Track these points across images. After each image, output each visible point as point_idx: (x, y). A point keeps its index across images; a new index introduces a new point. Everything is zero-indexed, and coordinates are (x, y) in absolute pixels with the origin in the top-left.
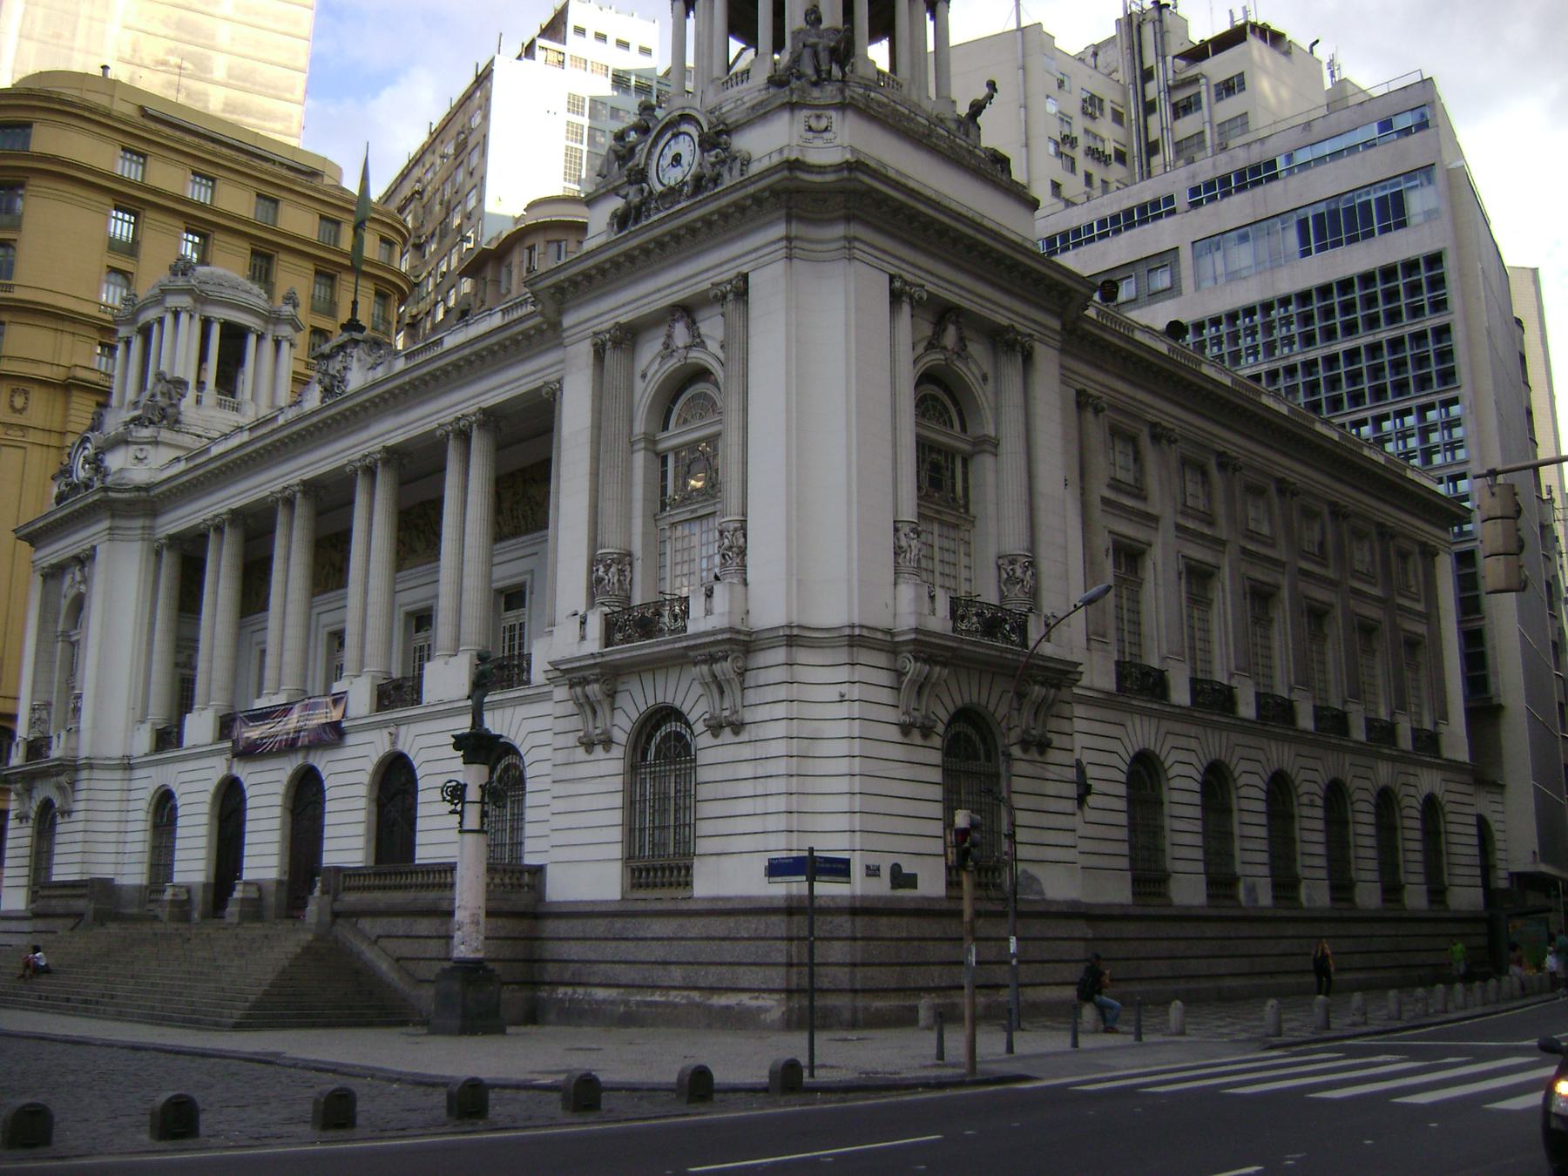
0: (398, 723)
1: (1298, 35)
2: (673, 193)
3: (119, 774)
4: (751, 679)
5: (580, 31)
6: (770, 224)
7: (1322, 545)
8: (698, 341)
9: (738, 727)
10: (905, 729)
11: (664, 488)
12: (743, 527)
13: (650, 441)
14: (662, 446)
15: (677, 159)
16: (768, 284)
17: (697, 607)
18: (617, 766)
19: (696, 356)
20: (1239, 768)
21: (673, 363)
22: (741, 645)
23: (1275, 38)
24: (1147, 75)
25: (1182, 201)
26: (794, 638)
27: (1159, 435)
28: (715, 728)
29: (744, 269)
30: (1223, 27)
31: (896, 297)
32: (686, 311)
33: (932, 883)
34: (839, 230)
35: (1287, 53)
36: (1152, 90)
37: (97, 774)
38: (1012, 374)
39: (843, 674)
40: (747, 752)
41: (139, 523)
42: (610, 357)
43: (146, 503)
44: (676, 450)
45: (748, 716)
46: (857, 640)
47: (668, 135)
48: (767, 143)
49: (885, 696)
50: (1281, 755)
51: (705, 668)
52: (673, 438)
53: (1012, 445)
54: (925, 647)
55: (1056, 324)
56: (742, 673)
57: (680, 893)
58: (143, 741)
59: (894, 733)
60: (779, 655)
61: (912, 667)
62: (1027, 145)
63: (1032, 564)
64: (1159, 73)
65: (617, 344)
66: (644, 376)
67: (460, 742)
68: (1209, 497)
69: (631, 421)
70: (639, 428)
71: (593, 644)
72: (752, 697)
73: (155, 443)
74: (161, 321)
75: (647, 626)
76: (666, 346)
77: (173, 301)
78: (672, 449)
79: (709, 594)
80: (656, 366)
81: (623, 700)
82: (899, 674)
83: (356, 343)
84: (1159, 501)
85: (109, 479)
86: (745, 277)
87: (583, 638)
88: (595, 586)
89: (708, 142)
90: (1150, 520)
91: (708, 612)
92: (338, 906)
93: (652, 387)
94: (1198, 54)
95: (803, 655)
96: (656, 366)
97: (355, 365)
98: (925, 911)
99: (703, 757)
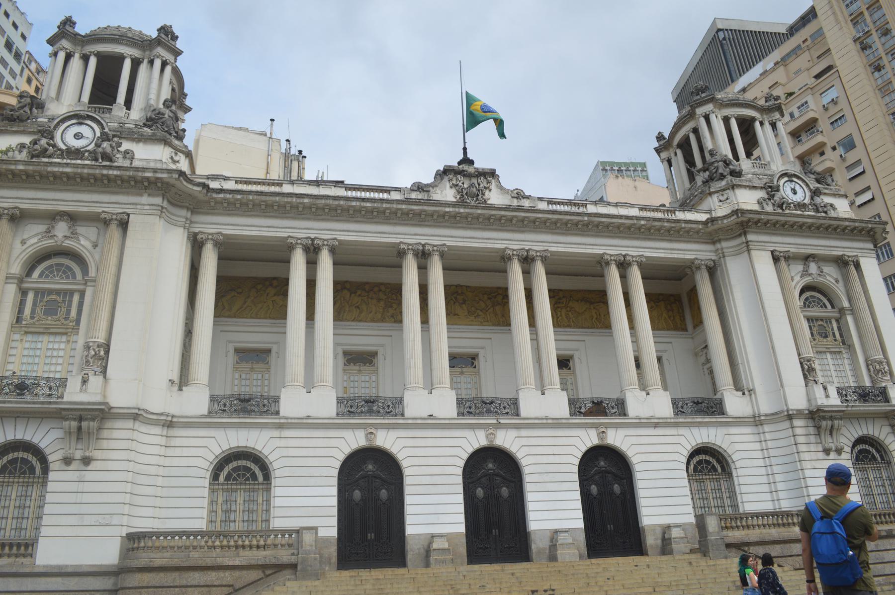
4: (105, 434)
6: (157, 196)
8: (74, 235)
11: (21, 311)
12: (107, 347)
13: (21, 281)
14: (25, 285)
15: (78, 136)
19: (68, 243)
21: (48, 243)
22: (102, 414)
29: (129, 211)
32: (72, 218)
44: (37, 292)
45: (97, 454)
47: (74, 121)
51: (74, 424)
56: (100, 429)
57: (26, 561)
66: (23, 242)
72: (105, 444)
76: (48, 231)
78: (33, 289)
79: (85, 382)
80: (35, 240)
86: (128, 215)
93: (30, 251)
96: (35, 240)
99: (52, 476)
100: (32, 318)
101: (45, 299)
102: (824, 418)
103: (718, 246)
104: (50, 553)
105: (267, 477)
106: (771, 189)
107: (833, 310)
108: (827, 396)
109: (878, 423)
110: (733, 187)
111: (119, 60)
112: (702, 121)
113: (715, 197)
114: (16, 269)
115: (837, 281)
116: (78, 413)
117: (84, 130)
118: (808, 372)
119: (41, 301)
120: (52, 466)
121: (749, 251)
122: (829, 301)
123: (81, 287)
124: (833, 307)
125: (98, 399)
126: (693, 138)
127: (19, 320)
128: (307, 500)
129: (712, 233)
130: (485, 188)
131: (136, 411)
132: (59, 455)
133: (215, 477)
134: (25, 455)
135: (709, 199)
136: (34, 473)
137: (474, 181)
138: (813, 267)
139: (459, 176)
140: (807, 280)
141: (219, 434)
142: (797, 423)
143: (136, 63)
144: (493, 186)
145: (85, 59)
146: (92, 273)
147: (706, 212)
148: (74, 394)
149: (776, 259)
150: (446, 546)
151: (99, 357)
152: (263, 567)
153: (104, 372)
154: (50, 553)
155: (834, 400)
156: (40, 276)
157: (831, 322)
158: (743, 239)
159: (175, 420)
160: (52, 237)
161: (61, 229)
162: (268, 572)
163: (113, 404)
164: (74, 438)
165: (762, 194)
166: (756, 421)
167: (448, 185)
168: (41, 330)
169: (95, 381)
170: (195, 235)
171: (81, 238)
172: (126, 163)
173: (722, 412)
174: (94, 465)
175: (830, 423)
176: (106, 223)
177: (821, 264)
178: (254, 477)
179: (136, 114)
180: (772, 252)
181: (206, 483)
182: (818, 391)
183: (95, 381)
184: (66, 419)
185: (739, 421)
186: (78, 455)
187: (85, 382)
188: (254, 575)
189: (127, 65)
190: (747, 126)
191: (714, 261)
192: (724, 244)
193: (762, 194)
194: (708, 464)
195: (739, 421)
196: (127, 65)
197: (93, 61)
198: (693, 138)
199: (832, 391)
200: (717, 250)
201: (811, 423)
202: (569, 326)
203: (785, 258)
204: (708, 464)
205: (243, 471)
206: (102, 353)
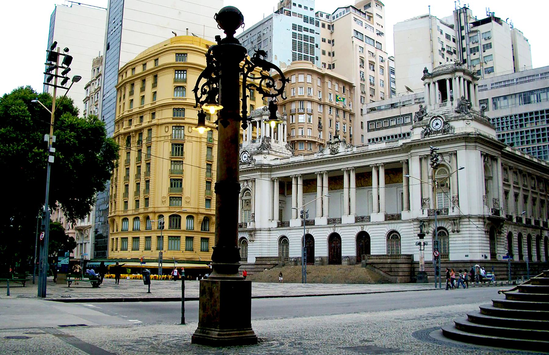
0: (363, 225)
1: (503, 18)
2: (437, 132)
3: (267, 232)
4: (461, 223)
5: (295, 4)
7: (535, 185)
9: (458, 231)
10: (485, 231)
15: (437, 124)
16: (462, 154)
17: (450, 210)
18: (431, 237)
19: (443, 163)
20: (523, 233)
23: (497, 20)
24: (462, 28)
25: (489, 87)
26: (469, 217)
27: (511, 168)
28: (453, 231)
30: (485, 17)
31: (481, 155)
33: (489, 258)
34: (473, 144)
35: (501, 24)
36: (463, 33)
37: (262, 232)
38: (494, 164)
39: (478, 223)
40: (460, 236)
41: (267, 173)
42: (423, 160)
43: (270, 169)
46: (481, 218)
48: (460, 127)
49: (482, 226)
50: (529, 231)
53: (495, 178)
54: (489, 218)
55: (500, 153)
58: (274, 224)
59: (484, 232)
61: (487, 222)
62: (432, 52)
63: (498, 201)
64: (465, 28)
65: (425, 158)
67: (419, 235)
68: (518, 179)
69: (428, 173)
70: (430, 174)
71: (426, 215)
72: (461, 226)
73: (269, 154)
74: (260, 122)
77: (264, 117)
79: (453, 208)
81: (432, 225)
82: (485, 222)
83: (340, 142)
84: (511, 182)
85: (256, 162)
88: (423, 204)
89: (445, 123)
90: (509, 185)
91: (453, 212)
92: (367, 262)
94: (477, 23)
95: (471, 220)
97: (340, 146)
98: (488, 262)
99: (450, 236)
104: (453, 257)
111: (444, 81)
117: (438, 121)
120: (450, 234)
132: (451, 230)
143: (451, 80)
145: (434, 83)
148: (451, 213)
151: (456, 201)
154: (453, 257)
174: (460, 233)
176: (451, 154)
179: (455, 103)
187: (453, 208)
189: (448, 82)
196: (448, 82)
197: (437, 84)
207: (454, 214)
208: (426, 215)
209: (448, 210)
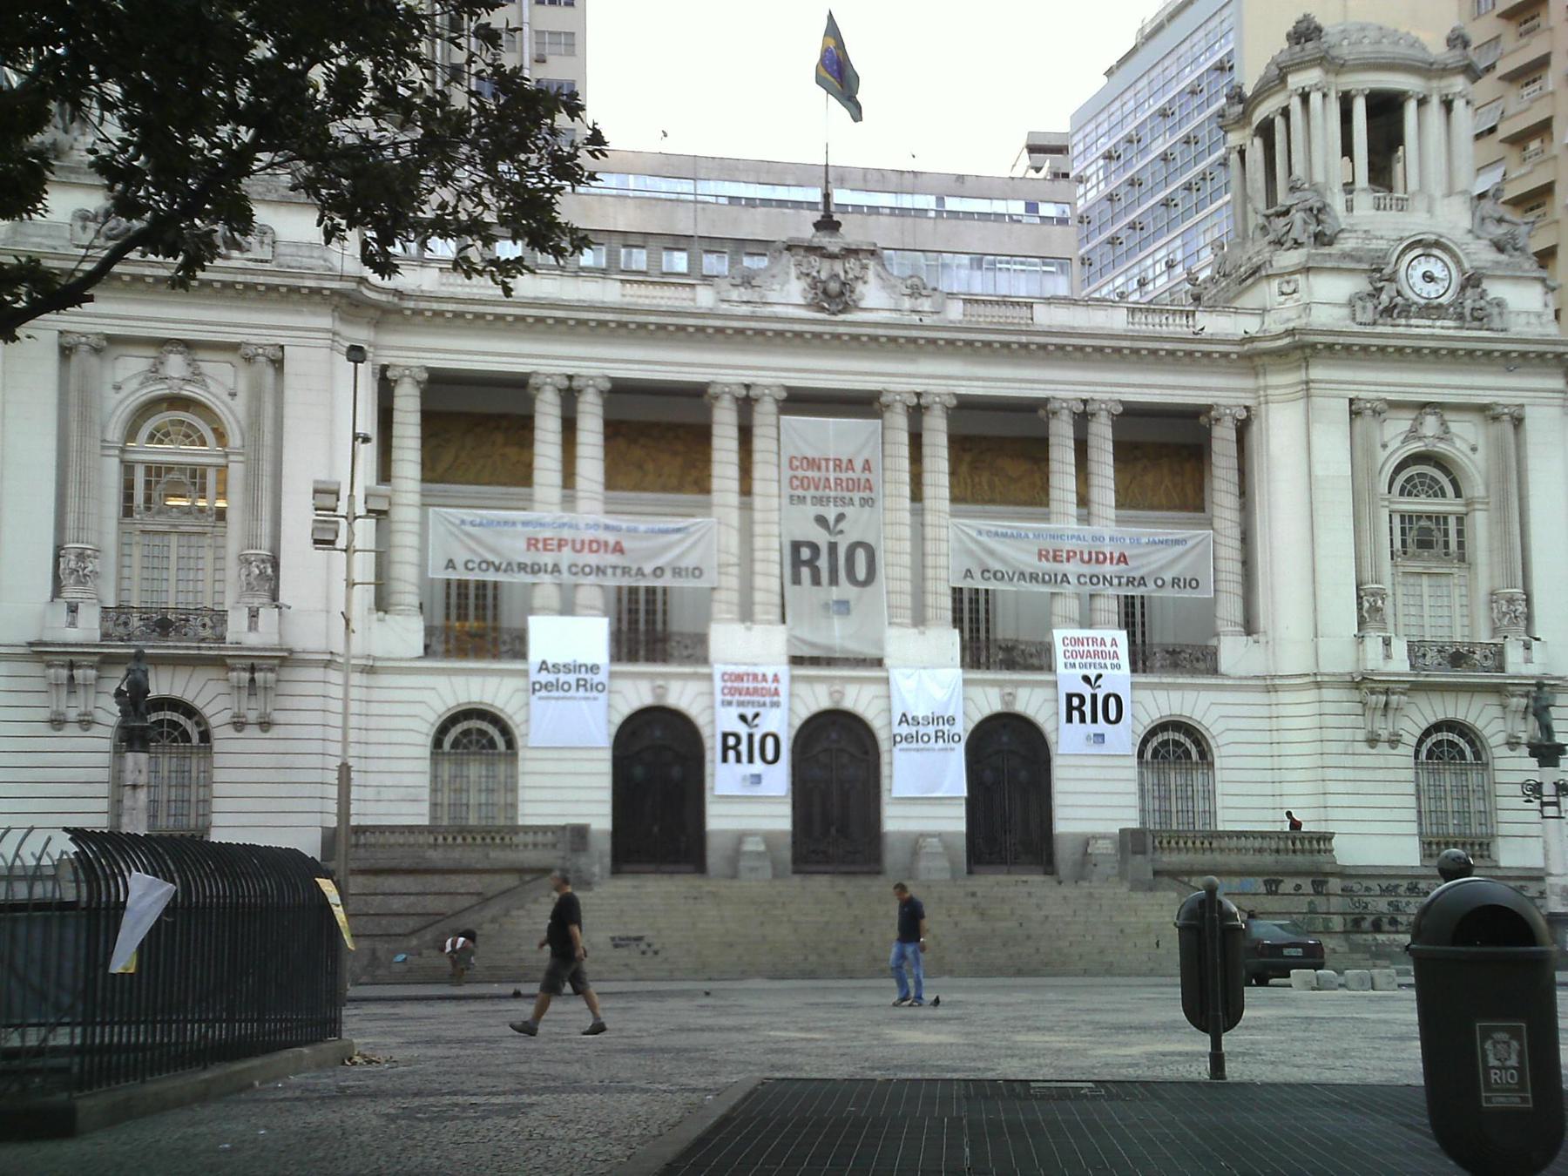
8: (196, 377)
9: (265, 725)
18: (107, 745)
19: (190, 391)
22: (286, 659)
28: (239, 725)
29: (281, 341)
45: (278, 717)
52: (147, 452)
60: (317, 673)
72: (288, 703)
75: (163, 626)
79: (254, 615)
86: (282, 347)
87: (72, 624)
96: (134, 384)
99: (217, 746)
100: (148, 509)
101: (164, 480)
102: (1373, 692)
103: (1262, 382)
105: (510, 743)
106: (1379, 271)
107: (1459, 500)
108: (1388, 657)
109: (1479, 701)
110: (1307, 270)
112: (1296, 105)
113: (1275, 283)
114: (115, 433)
115: (1474, 449)
116: (249, 662)
118: (1369, 612)
119: (157, 483)
120: (216, 733)
121: (1308, 396)
122: (1455, 484)
123: (221, 461)
124: (1458, 494)
125: (273, 640)
126: (1279, 123)
127: (128, 511)
128: (566, 780)
129: (1251, 358)
130: (857, 278)
131: (328, 657)
132: (226, 716)
133: (438, 743)
134: (176, 717)
135: (1264, 285)
136: (189, 741)
137: (838, 267)
138: (1431, 424)
139: (812, 258)
140: (1415, 447)
141: (441, 682)
142: (1328, 694)
144: (870, 275)
146: (235, 440)
147: (1251, 312)
149: (1355, 413)
150: (762, 848)
152: (520, 871)
153: (274, 596)
155: (1400, 663)
156: (151, 438)
157: (1446, 522)
158: (1300, 376)
159: (378, 664)
160: (164, 379)
161: (176, 364)
162: (528, 878)
163: (298, 646)
164: (245, 693)
165: (1360, 284)
166: (1270, 684)
167: (793, 272)
168: (166, 529)
169: (267, 616)
170: (384, 368)
171: (209, 381)
172: (266, 253)
173: (1214, 671)
174: (274, 732)
175: (1383, 698)
177: (1448, 416)
178: (492, 744)
180: (1351, 401)
181: (426, 752)
182: (1374, 645)
183: (267, 616)
184: (233, 670)
185: (1243, 684)
186: (252, 716)
187: (254, 615)
188: (510, 881)
190: (1386, 112)
191: (1247, 408)
192: (1273, 380)
193: (1360, 284)
194: (1176, 749)
195: (1243, 684)
198: (1279, 123)
199: (1400, 648)
200: (1257, 390)
201: (1356, 695)
202: (992, 501)
203: (1374, 411)
204: (1176, 749)
205: (475, 737)
206: (269, 571)
207: (252, 640)
208: (88, 628)
209: (220, 617)
